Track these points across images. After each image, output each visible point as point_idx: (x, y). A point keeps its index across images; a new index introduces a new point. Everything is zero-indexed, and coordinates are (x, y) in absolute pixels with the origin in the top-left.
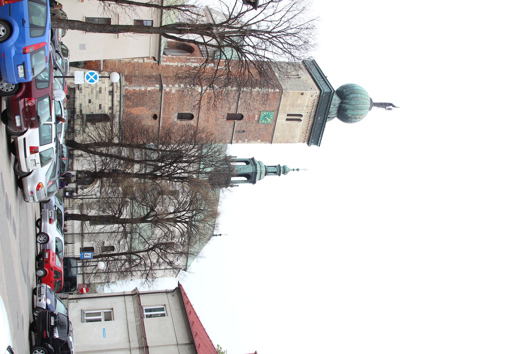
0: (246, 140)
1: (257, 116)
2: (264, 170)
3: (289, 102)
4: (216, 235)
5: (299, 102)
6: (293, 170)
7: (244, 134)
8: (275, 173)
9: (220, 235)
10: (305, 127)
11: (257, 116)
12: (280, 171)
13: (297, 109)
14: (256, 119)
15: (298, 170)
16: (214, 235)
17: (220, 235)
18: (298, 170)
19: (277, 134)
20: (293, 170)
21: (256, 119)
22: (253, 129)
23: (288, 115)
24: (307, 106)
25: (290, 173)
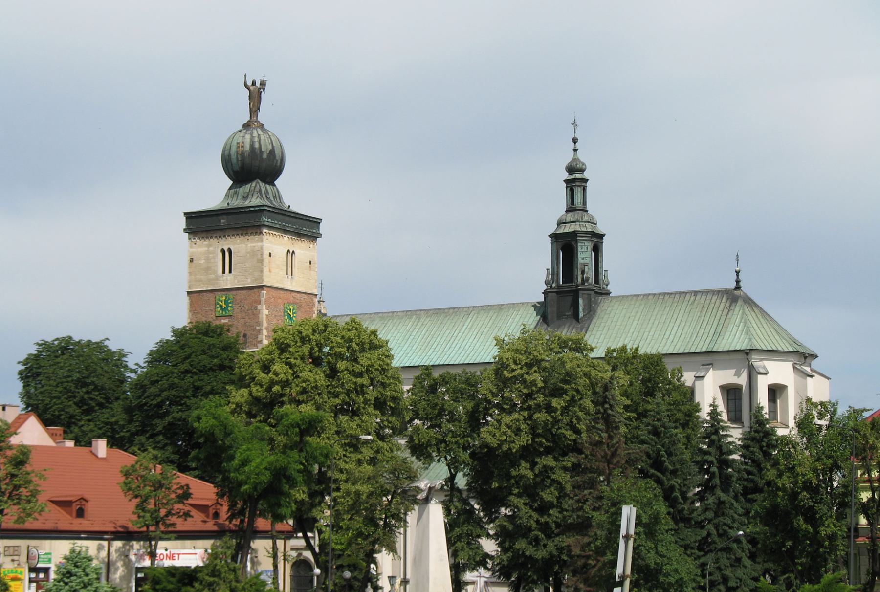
0: (258, 328)
1: (223, 321)
2: (570, 216)
3: (203, 277)
4: (738, 282)
5: (202, 261)
6: (575, 150)
7: (248, 334)
8: (584, 189)
9: (738, 273)
10: (238, 239)
11: (223, 321)
12: (576, 182)
13: (212, 261)
14: (226, 321)
15: (575, 141)
16: (738, 288)
17: (738, 273)
18: (575, 141)
19: (249, 280)
20: (575, 150)
21: (226, 321)
22: (242, 321)
23: (224, 272)
24: (209, 246)
25: (582, 156)
